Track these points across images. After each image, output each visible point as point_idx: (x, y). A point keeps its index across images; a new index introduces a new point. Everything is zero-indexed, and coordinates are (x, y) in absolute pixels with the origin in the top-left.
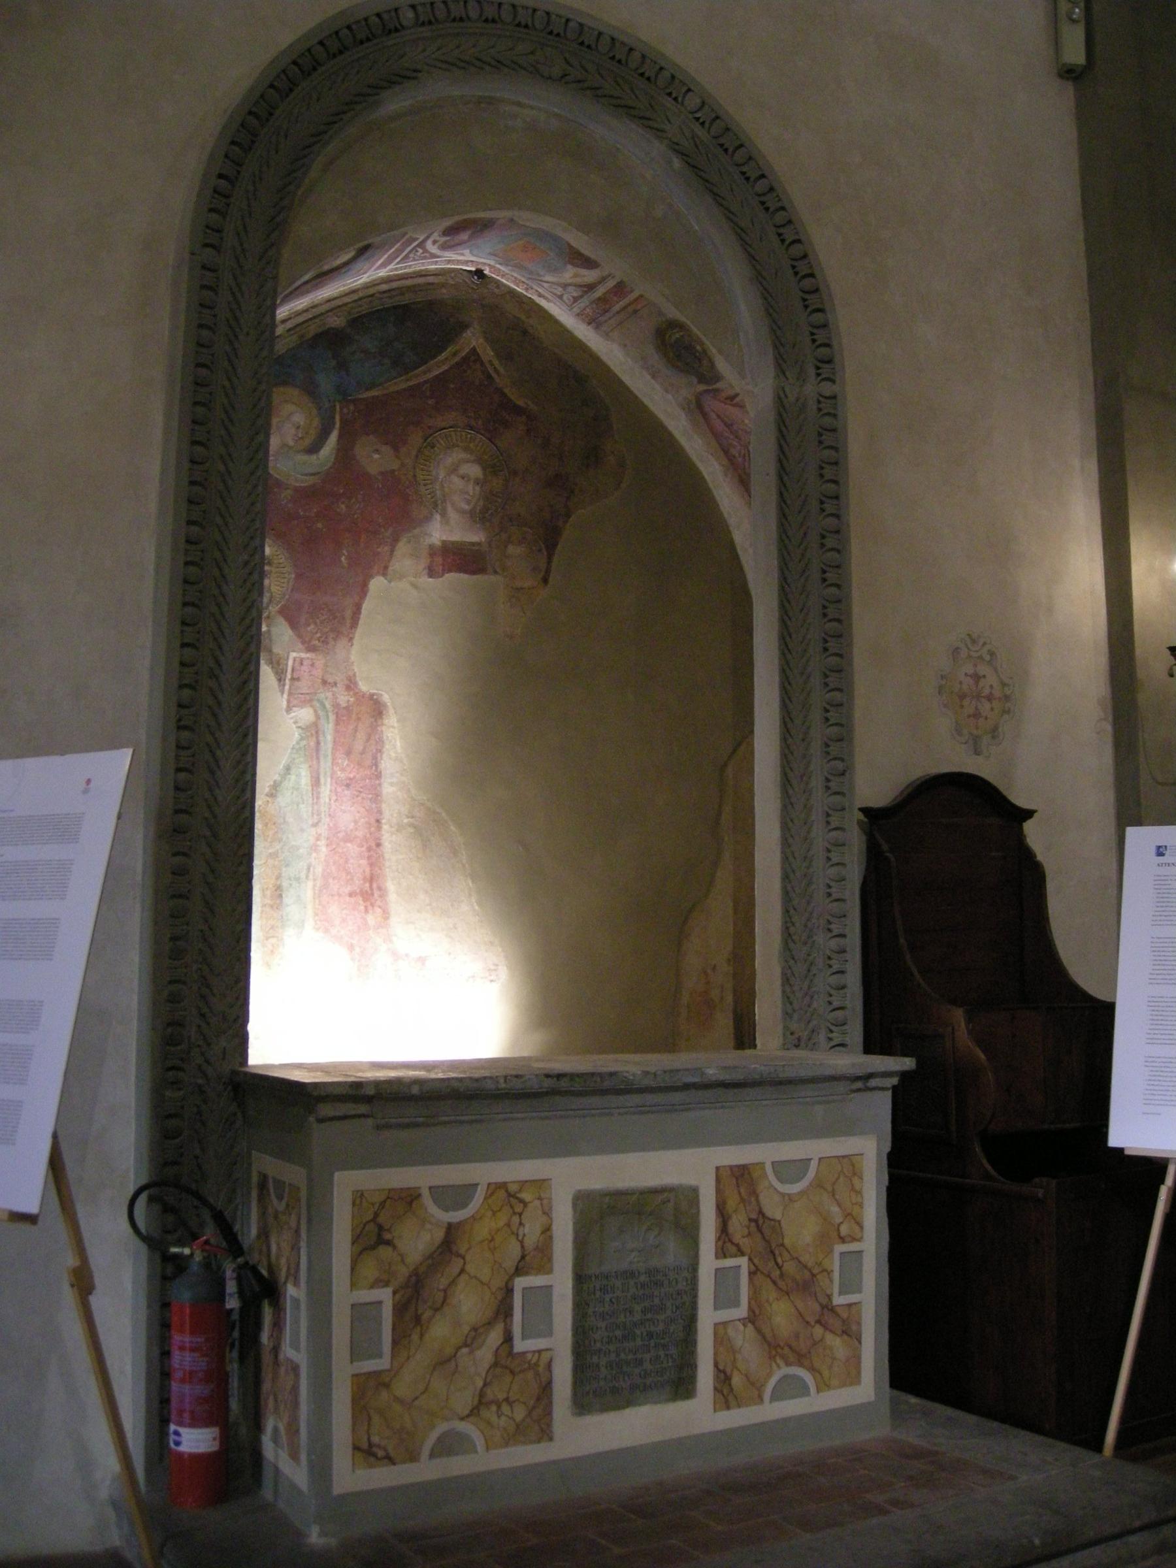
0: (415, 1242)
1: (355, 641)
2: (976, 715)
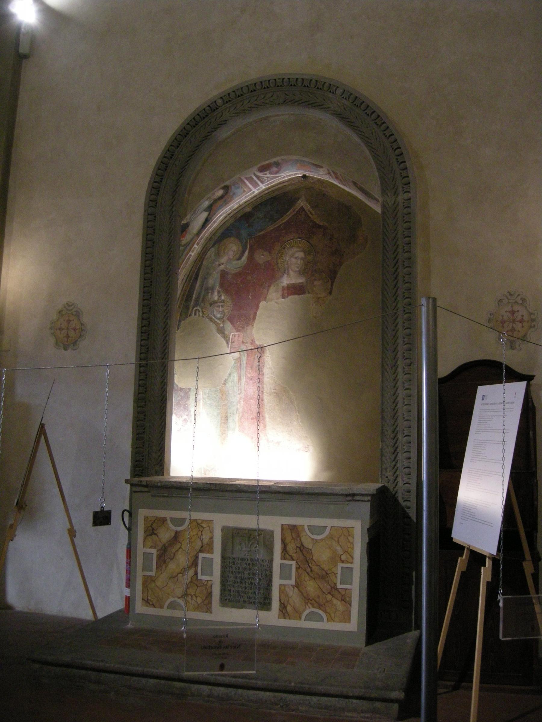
0: (165, 535)
2: (513, 330)
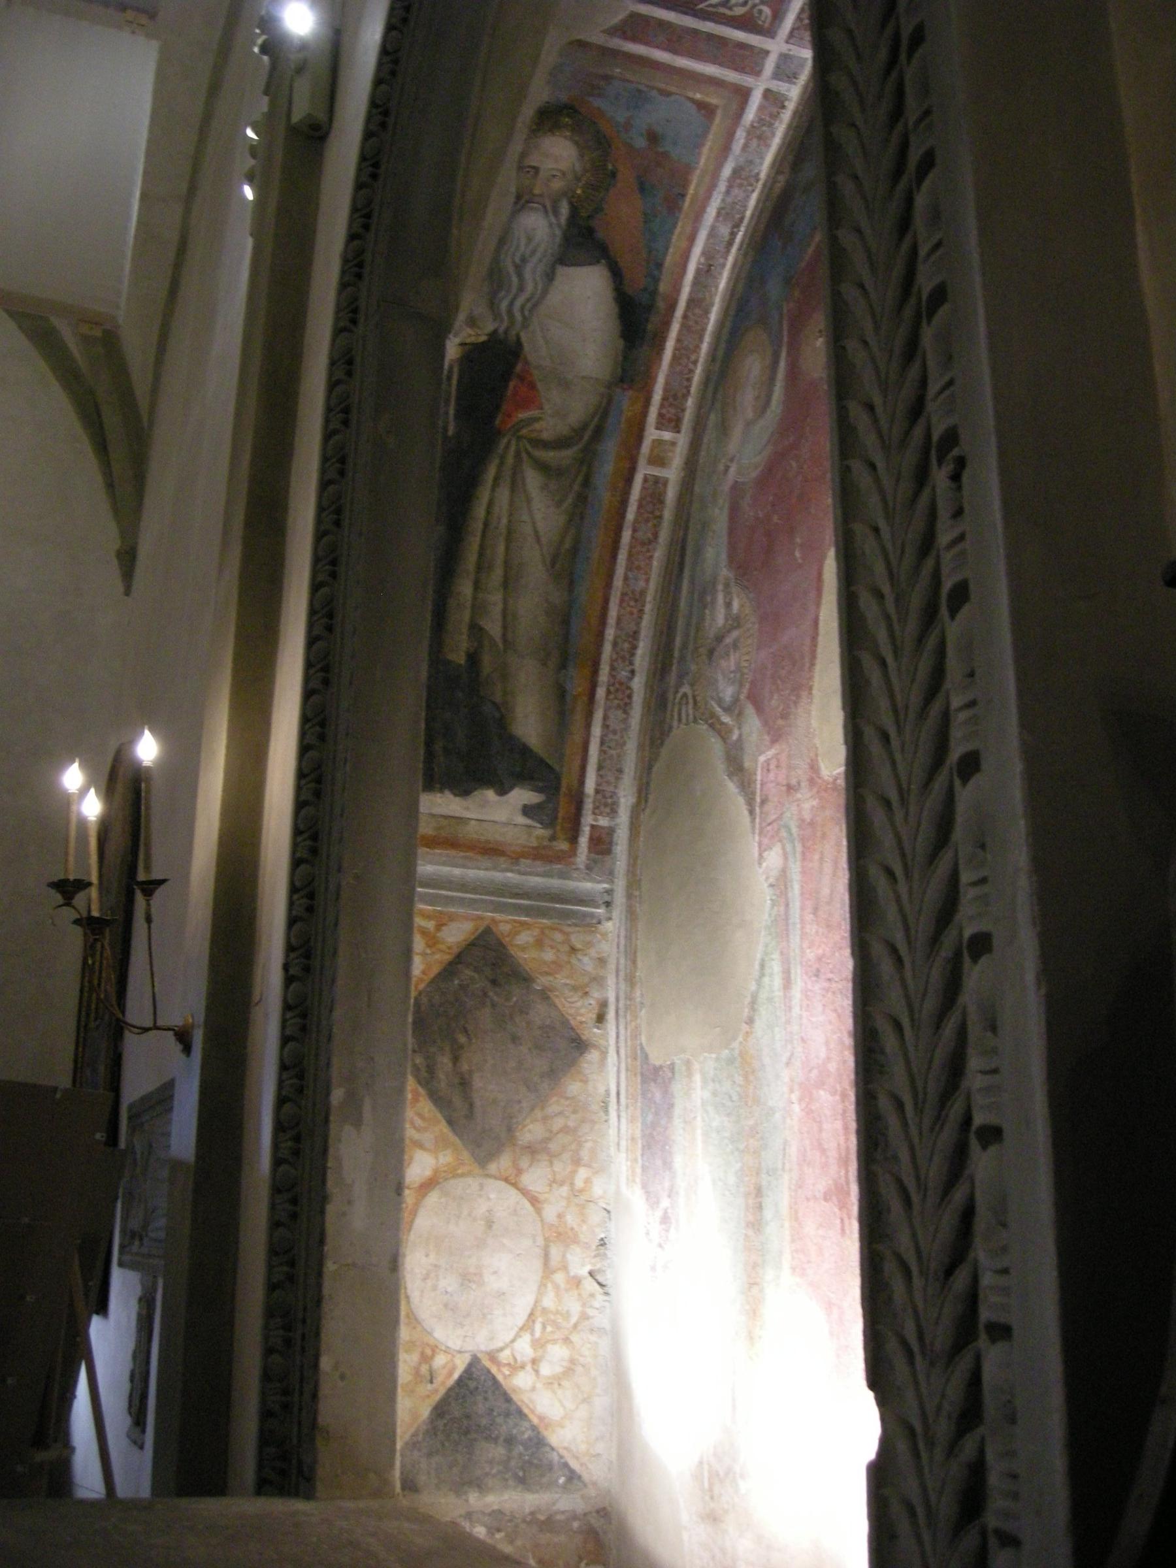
1: (814, 692)
